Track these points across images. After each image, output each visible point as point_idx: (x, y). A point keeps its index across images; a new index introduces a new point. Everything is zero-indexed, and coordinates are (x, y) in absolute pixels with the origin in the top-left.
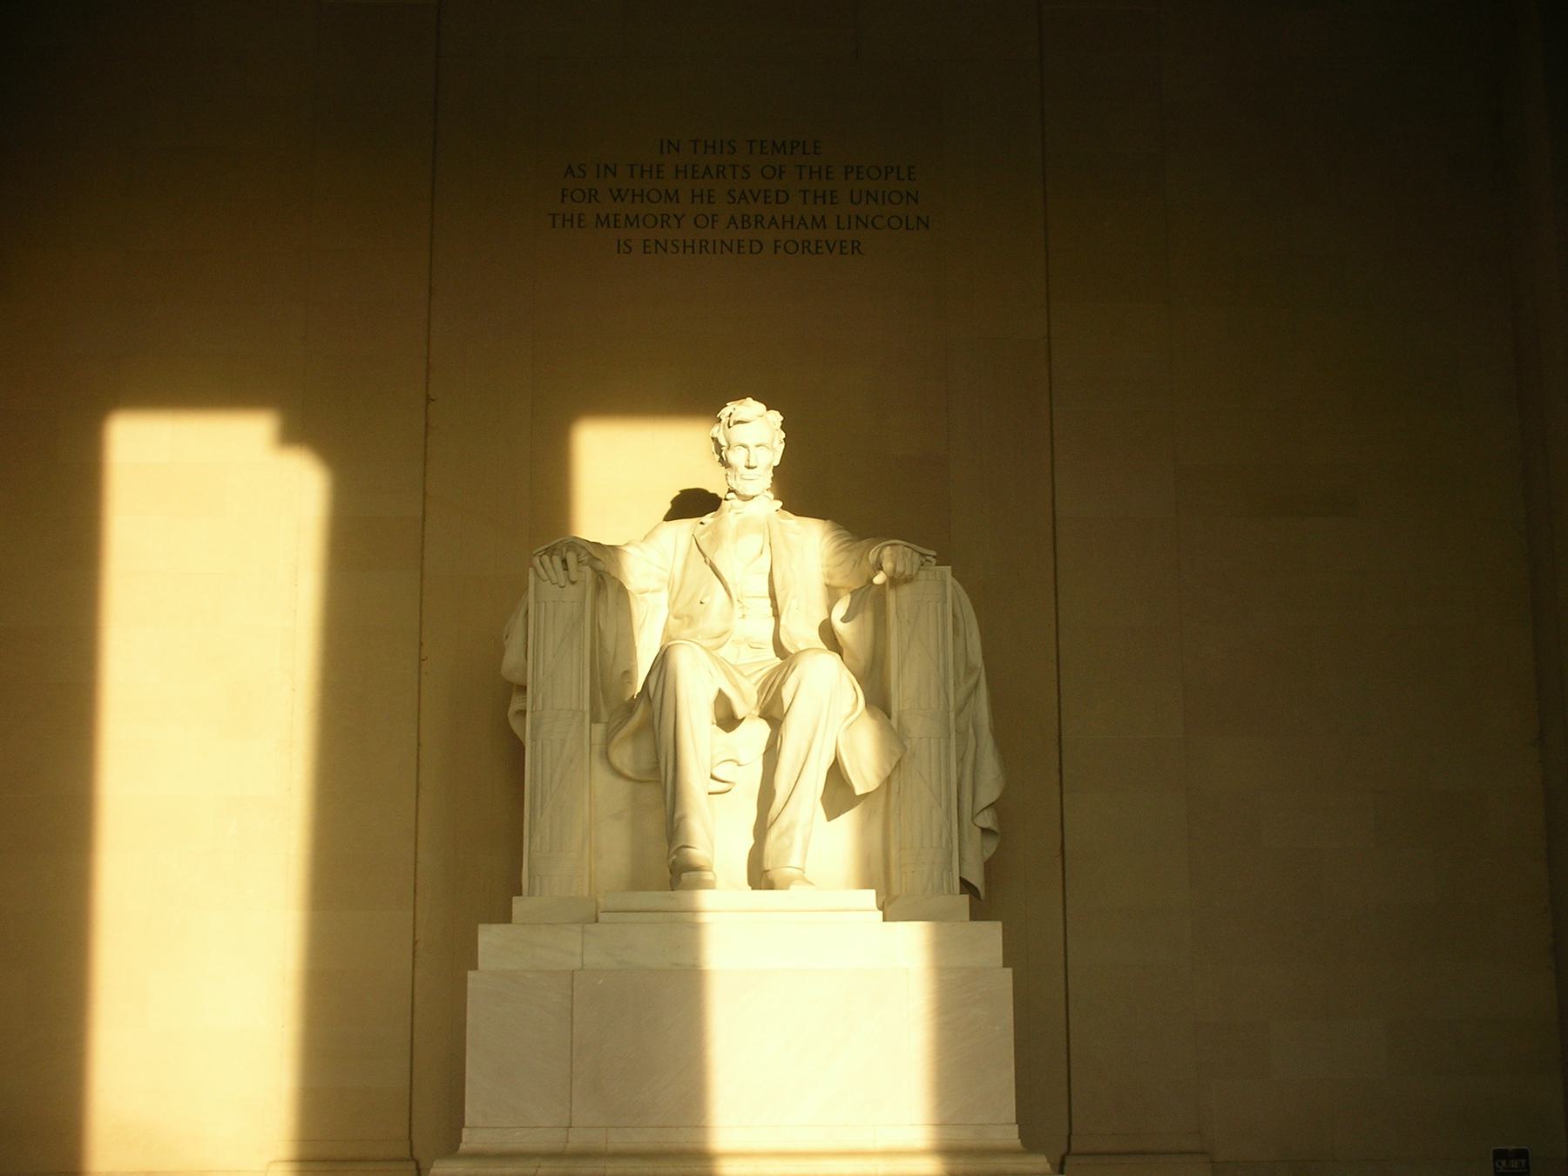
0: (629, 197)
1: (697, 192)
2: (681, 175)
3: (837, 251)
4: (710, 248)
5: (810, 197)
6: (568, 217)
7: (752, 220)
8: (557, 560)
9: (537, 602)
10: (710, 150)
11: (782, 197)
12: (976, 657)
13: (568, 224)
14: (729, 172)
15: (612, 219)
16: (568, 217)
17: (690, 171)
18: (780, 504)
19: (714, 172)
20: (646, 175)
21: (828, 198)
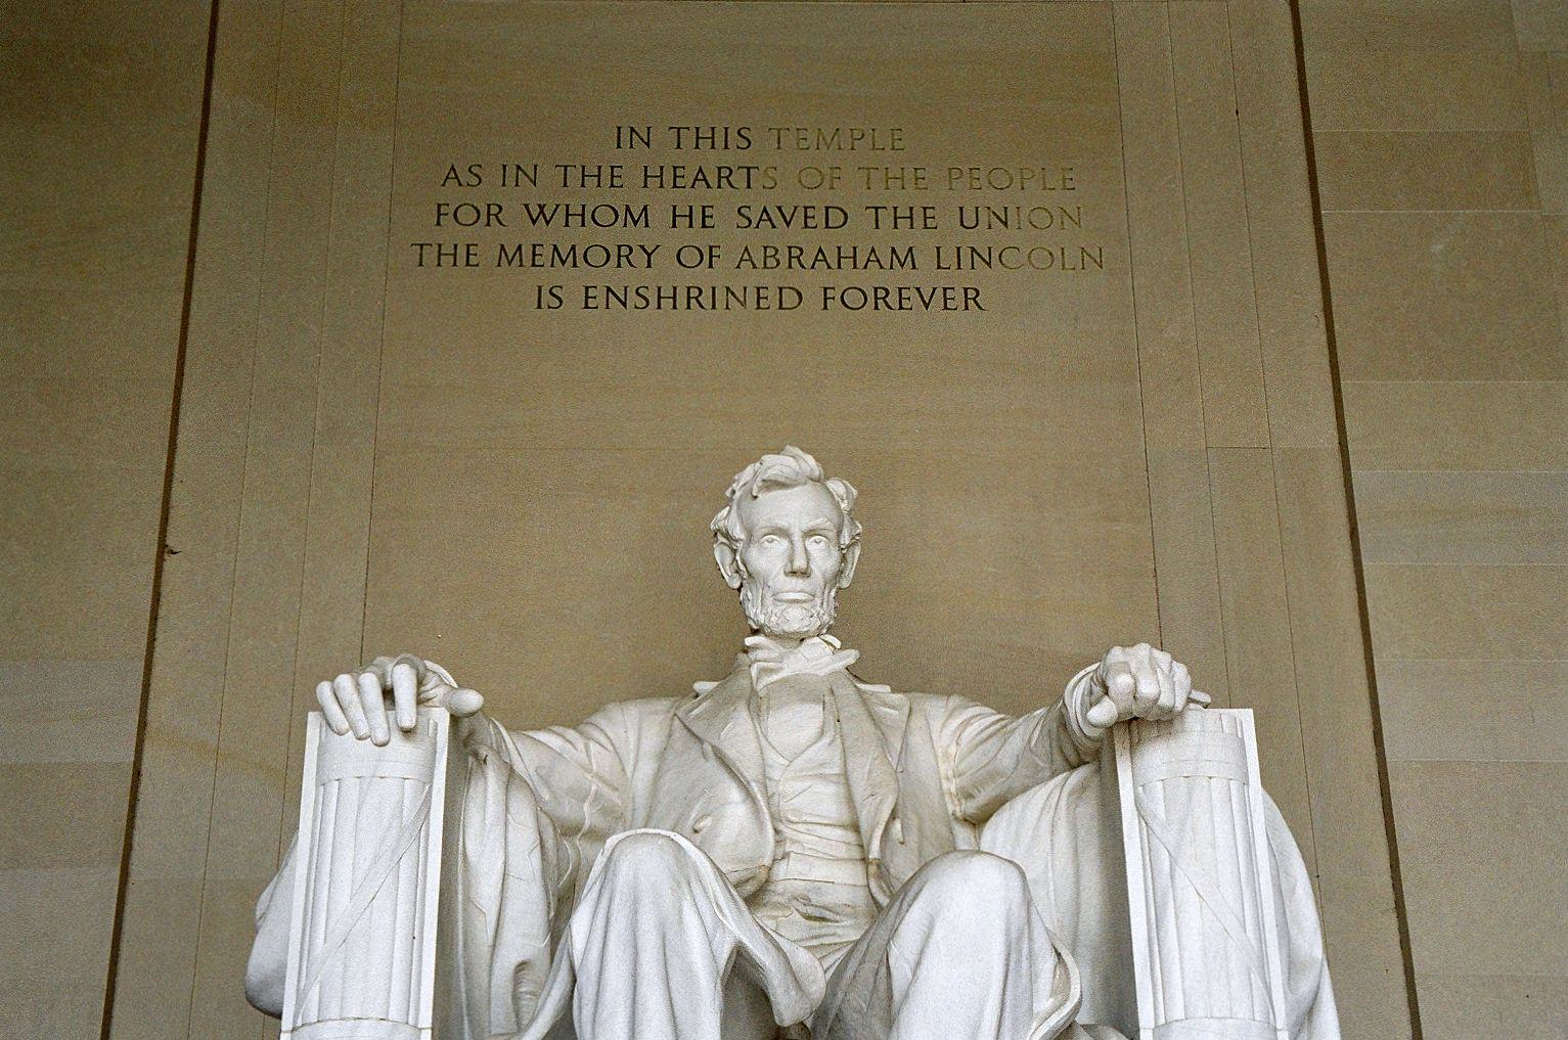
1: (683, 210)
2: (653, 183)
4: (706, 299)
5: (886, 218)
6: (447, 249)
8: (370, 681)
9: (321, 783)
10: (705, 144)
11: (836, 218)
12: (1310, 941)
13: (447, 260)
14: (739, 178)
15: (527, 251)
16: (447, 249)
18: (851, 656)
19: (713, 180)
20: (591, 182)
21: (918, 221)
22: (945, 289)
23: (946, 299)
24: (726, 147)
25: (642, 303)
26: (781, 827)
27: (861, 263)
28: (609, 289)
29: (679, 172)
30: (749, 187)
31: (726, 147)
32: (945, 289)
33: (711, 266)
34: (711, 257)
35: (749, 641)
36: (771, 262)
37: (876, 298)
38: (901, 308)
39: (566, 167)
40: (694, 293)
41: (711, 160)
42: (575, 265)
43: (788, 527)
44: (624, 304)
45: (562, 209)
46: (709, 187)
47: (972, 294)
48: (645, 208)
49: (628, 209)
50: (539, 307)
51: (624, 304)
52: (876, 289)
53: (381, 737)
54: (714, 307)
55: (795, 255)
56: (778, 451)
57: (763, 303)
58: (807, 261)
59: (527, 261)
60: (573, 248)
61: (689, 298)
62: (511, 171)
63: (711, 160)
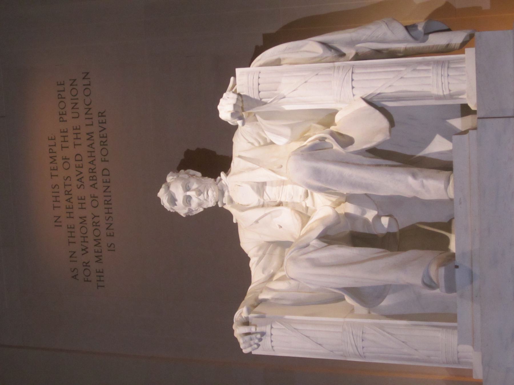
0: (85, 244)
1: (80, 206)
2: (72, 215)
3: (104, 126)
4: (108, 199)
5: (78, 142)
6: (98, 278)
7: (92, 175)
10: (58, 199)
11: (79, 158)
13: (102, 278)
14: (68, 188)
16: (98, 278)
17: (70, 210)
18: (222, 174)
19: (69, 196)
20: (73, 234)
22: (99, 123)
23: (102, 123)
24: (58, 192)
25: (110, 219)
26: (278, 202)
27: (93, 150)
28: (107, 229)
29: (68, 207)
30: (71, 185)
31: (58, 192)
32: (99, 123)
33: (97, 197)
34: (94, 197)
35: (220, 205)
36: (94, 178)
37: (104, 145)
38: (106, 137)
39: (69, 242)
40: (106, 202)
41: (63, 198)
42: (100, 240)
43: (183, 195)
44: (111, 224)
45: (83, 244)
46: (72, 198)
47: (100, 114)
48: (80, 218)
49: (81, 223)
50: (114, 250)
51: (111, 224)
52: (101, 145)
53: (259, 336)
54: (110, 196)
55: (92, 171)
56: (159, 200)
57: (108, 181)
58: (92, 167)
59: (100, 254)
60: (95, 240)
61: (108, 204)
62: (72, 259)
63: (63, 198)
